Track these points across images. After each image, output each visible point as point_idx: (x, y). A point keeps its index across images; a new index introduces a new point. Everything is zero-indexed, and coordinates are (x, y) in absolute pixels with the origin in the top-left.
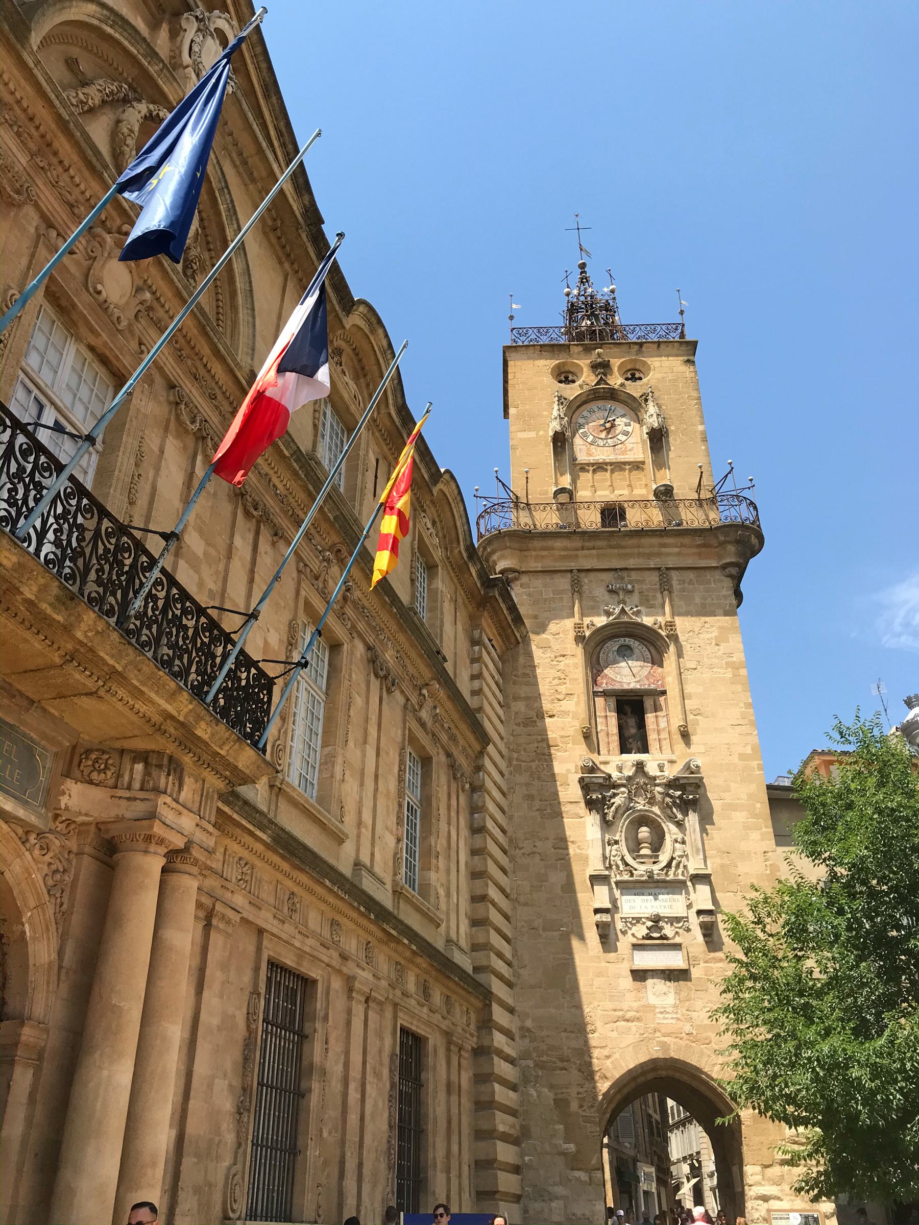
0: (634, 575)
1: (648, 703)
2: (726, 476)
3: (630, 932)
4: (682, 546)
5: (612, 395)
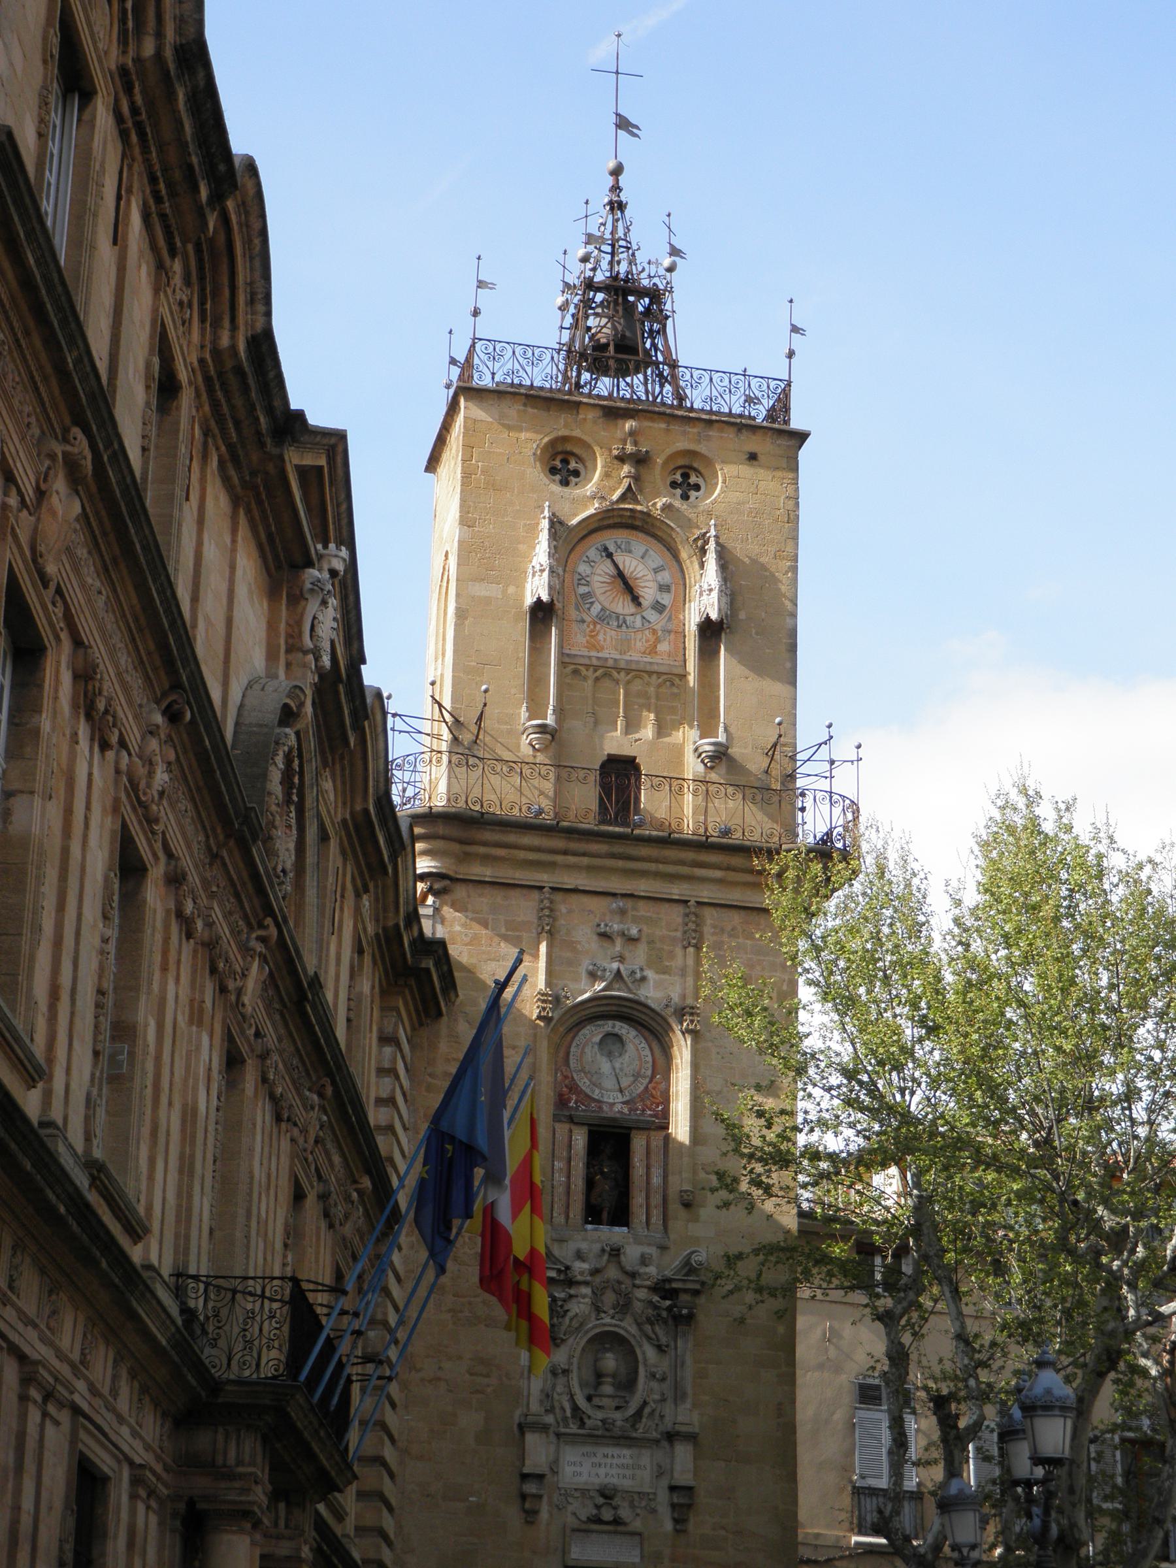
0: (644, 909)
1: (638, 1143)
2: (820, 745)
3: (570, 1508)
4: (728, 868)
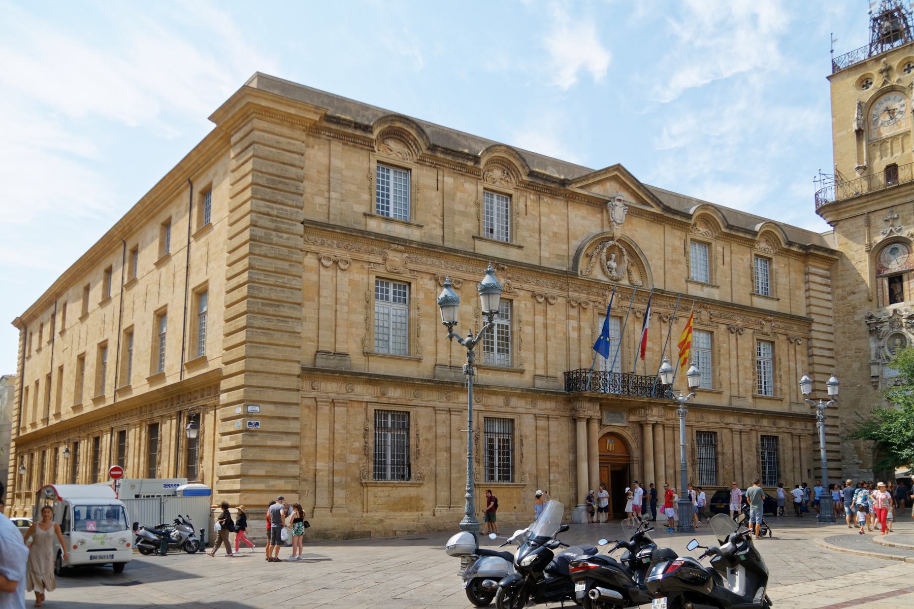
5: (893, 89)
